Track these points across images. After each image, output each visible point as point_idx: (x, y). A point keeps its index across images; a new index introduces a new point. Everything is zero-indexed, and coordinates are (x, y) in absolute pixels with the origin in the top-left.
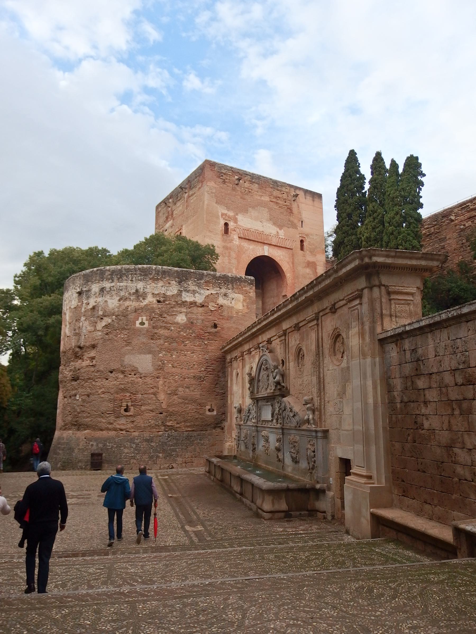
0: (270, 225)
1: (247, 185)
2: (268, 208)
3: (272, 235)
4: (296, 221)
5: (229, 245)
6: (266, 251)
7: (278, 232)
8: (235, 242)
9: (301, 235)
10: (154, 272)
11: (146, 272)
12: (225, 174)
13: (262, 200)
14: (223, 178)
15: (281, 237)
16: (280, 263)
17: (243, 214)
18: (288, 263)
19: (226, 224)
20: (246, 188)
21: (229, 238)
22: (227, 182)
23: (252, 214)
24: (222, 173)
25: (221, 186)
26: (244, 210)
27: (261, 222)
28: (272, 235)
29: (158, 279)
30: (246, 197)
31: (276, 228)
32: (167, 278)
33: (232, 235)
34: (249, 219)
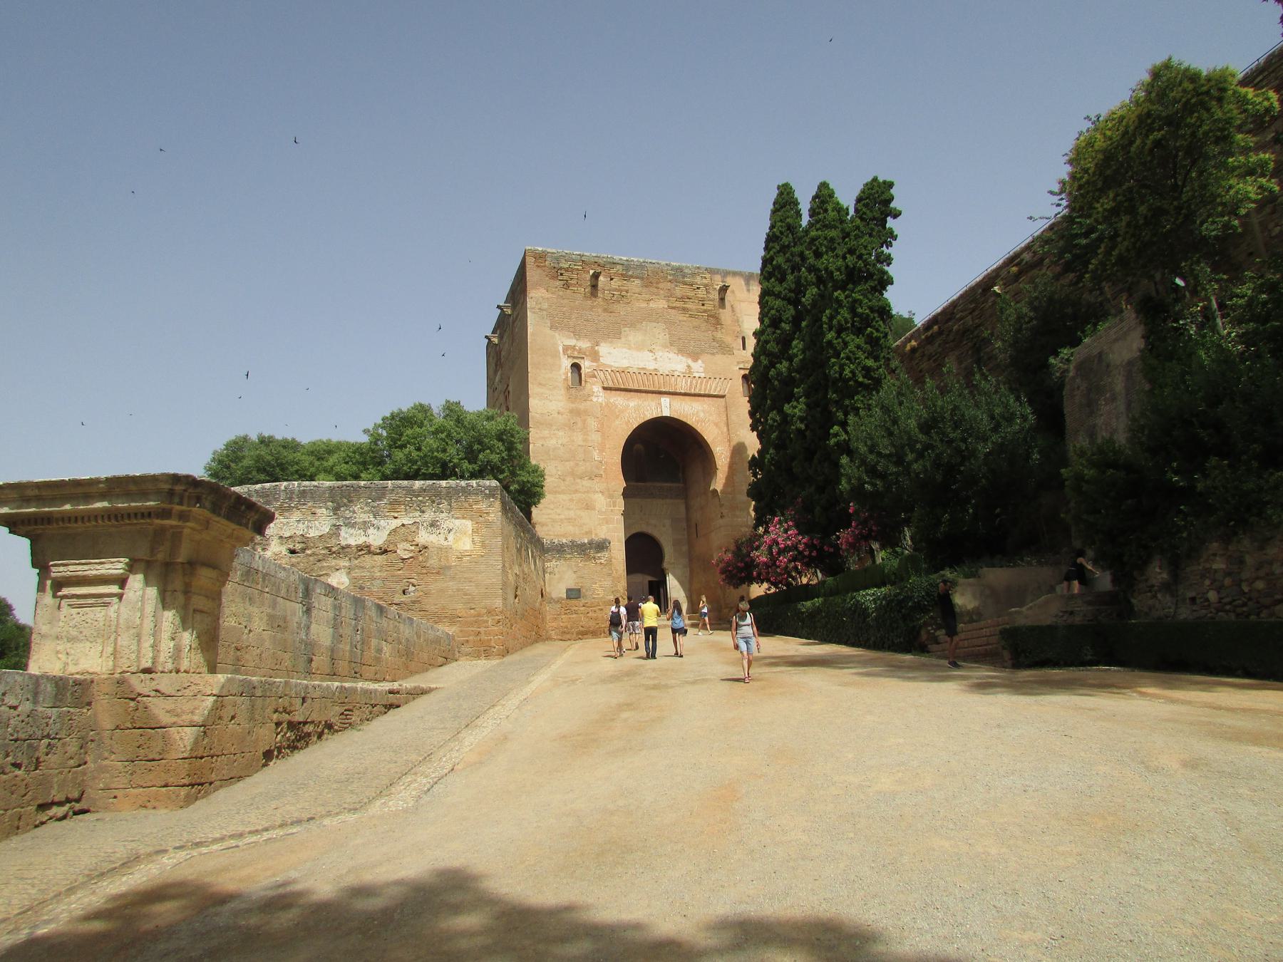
0: (671, 355)
1: (616, 283)
2: (665, 323)
3: (676, 374)
4: (728, 339)
5: (582, 406)
6: (666, 408)
7: (689, 366)
8: (595, 399)
9: (742, 366)
10: (283, 496)
11: (268, 496)
12: (567, 270)
13: (652, 309)
14: (565, 278)
15: (697, 375)
16: (699, 428)
17: (611, 342)
18: (716, 425)
19: (576, 367)
20: (615, 290)
21: (581, 393)
22: (572, 284)
23: (631, 338)
24: (561, 269)
25: (561, 293)
26: (613, 334)
27: (651, 351)
28: (676, 374)
29: (290, 509)
30: (616, 307)
31: (684, 359)
32: (310, 504)
33: (588, 386)
34: (625, 350)
